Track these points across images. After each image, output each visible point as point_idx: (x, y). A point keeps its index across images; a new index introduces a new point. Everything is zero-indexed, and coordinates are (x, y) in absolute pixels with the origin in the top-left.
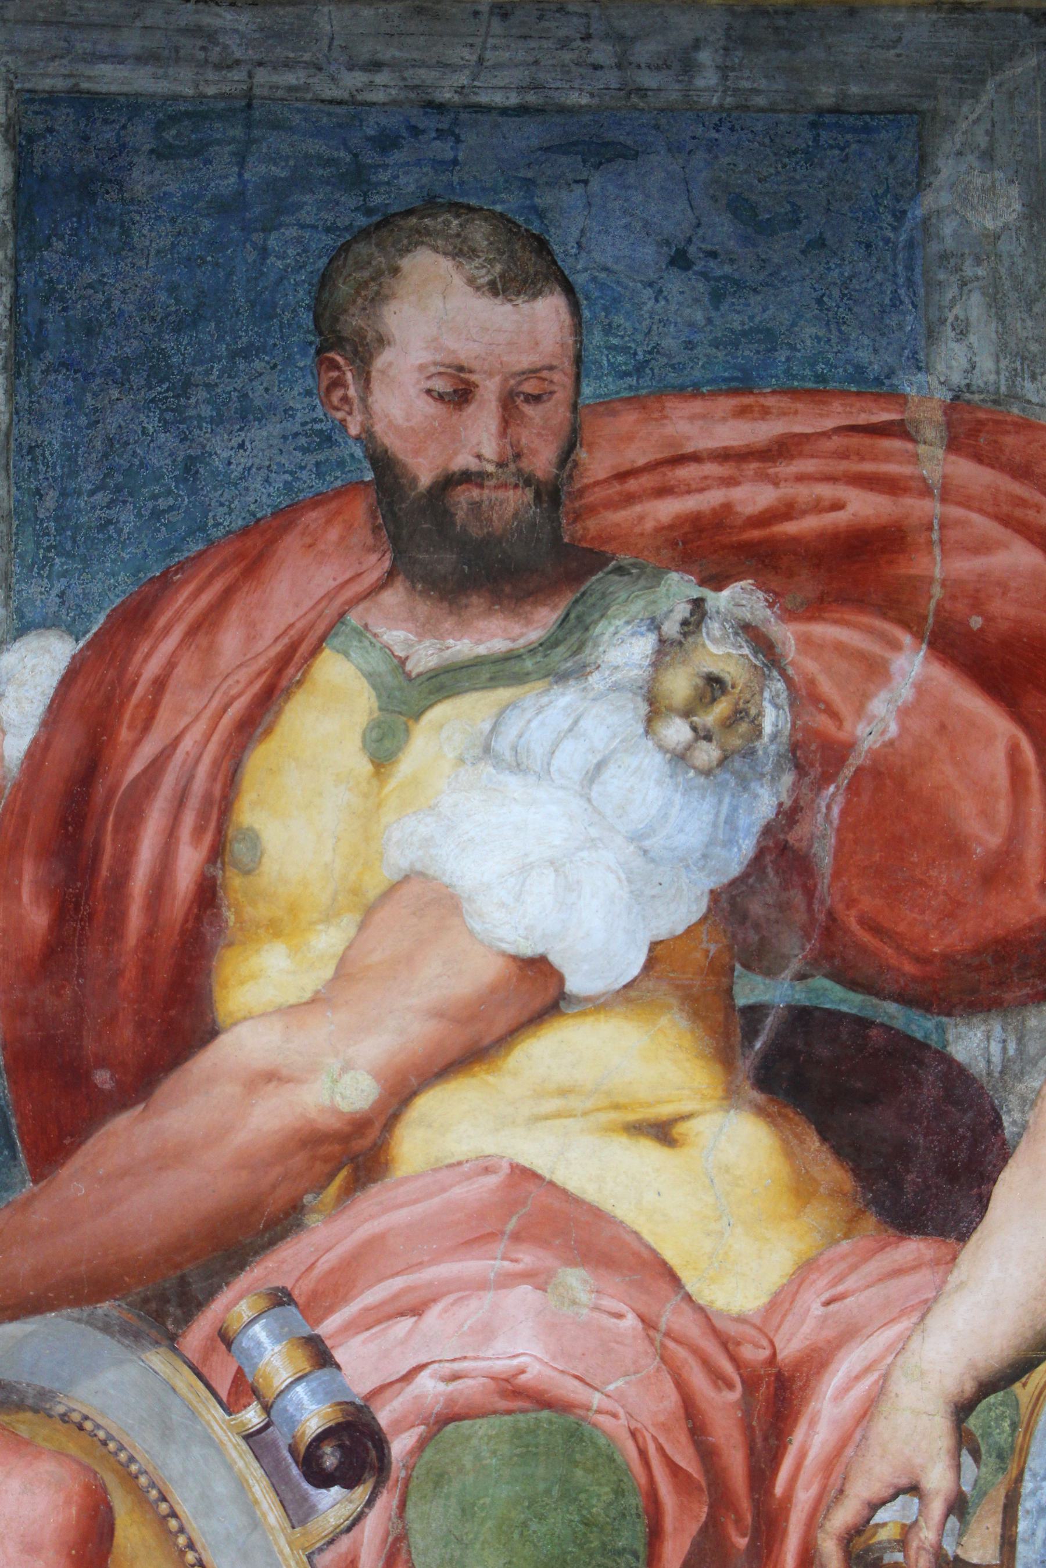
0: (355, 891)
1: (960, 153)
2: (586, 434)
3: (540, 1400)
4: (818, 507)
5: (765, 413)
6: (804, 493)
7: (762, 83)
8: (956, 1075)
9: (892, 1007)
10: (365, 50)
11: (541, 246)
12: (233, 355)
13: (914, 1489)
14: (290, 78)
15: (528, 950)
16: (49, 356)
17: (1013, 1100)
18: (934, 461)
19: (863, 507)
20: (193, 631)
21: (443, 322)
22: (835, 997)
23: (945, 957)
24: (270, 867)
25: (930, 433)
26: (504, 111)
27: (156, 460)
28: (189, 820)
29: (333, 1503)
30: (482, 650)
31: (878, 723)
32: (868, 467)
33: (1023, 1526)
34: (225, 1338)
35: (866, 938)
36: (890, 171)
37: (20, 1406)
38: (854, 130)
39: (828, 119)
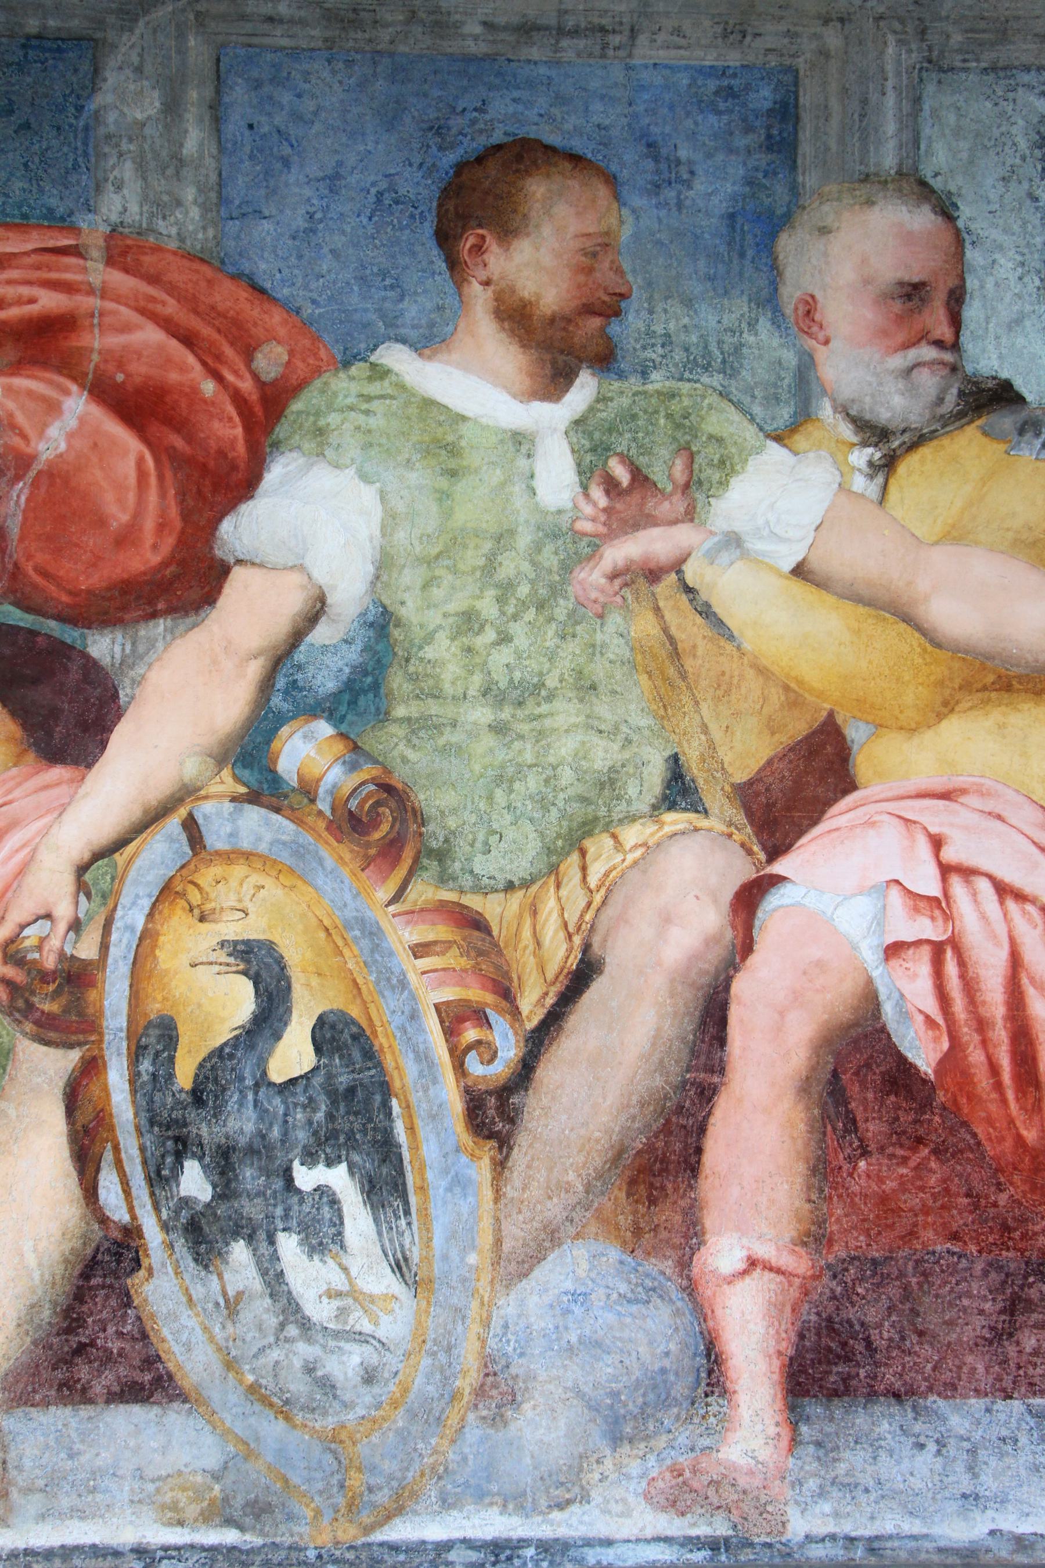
1: (120, 68)
4: (20, 302)
8: (91, 666)
9: (53, 623)
13: (48, 916)
17: (127, 682)
19: (49, 301)
23: (89, 592)
25: (95, 253)
32: (54, 275)
33: (114, 937)
36: (74, 79)
38: (50, 50)
39: (34, 42)
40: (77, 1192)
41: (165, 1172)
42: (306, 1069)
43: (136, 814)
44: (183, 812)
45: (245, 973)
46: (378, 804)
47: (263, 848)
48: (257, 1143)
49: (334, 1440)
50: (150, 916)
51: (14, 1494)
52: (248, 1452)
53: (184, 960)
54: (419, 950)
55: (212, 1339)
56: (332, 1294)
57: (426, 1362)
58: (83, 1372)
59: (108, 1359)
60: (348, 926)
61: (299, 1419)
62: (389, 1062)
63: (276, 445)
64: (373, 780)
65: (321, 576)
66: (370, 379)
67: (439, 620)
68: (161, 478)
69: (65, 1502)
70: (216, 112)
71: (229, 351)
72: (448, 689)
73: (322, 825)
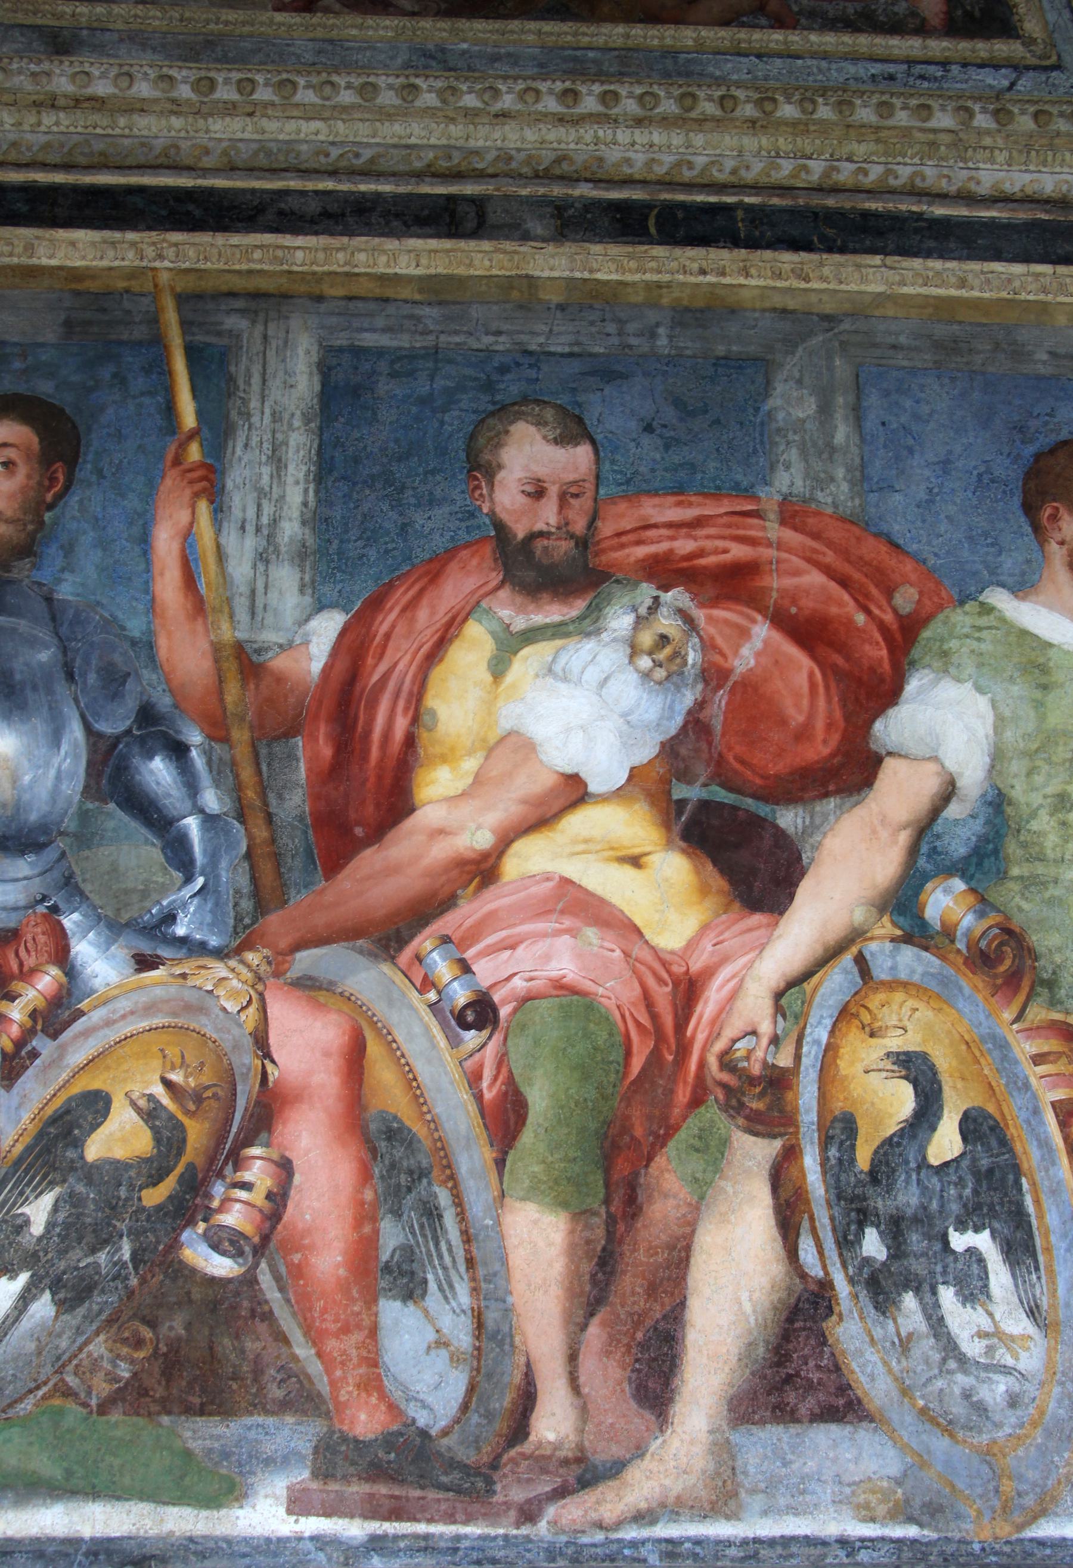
0: (484, 740)
2: (601, 514)
3: (573, 990)
4: (716, 552)
5: (690, 504)
6: (709, 544)
7: (689, 344)
8: (780, 835)
9: (750, 801)
10: (494, 326)
11: (580, 421)
12: (426, 473)
13: (754, 1033)
14: (457, 339)
15: (569, 770)
16: (336, 474)
17: (808, 847)
18: (773, 530)
19: (738, 552)
20: (404, 610)
21: (531, 459)
22: (721, 795)
23: (776, 776)
24: (441, 728)
26: (562, 355)
27: (387, 525)
28: (401, 704)
29: (471, 1038)
30: (548, 620)
31: (745, 659)
32: (741, 532)
33: (805, 1049)
34: (419, 959)
35: (737, 766)
37: (320, 988)
40: (782, 1253)
41: (851, 1237)
42: (956, 1154)
43: (819, 951)
44: (854, 950)
45: (906, 1078)
46: (1001, 944)
47: (916, 978)
48: (921, 1214)
49: (988, 1453)
50: (832, 1032)
51: (743, 1495)
52: (923, 1464)
53: (859, 1068)
54: (1038, 1059)
55: (890, 1371)
56: (982, 1335)
57: (1057, 1390)
58: (791, 1397)
59: (810, 1387)
60: (983, 1040)
61: (960, 1435)
62: (1018, 1148)
63: (912, 663)
64: (997, 925)
65: (951, 765)
66: (980, 614)
67: (1040, 801)
68: (827, 688)
69: (782, 1501)
70: (858, 414)
71: (874, 591)
72: (1049, 852)
73: (960, 960)
